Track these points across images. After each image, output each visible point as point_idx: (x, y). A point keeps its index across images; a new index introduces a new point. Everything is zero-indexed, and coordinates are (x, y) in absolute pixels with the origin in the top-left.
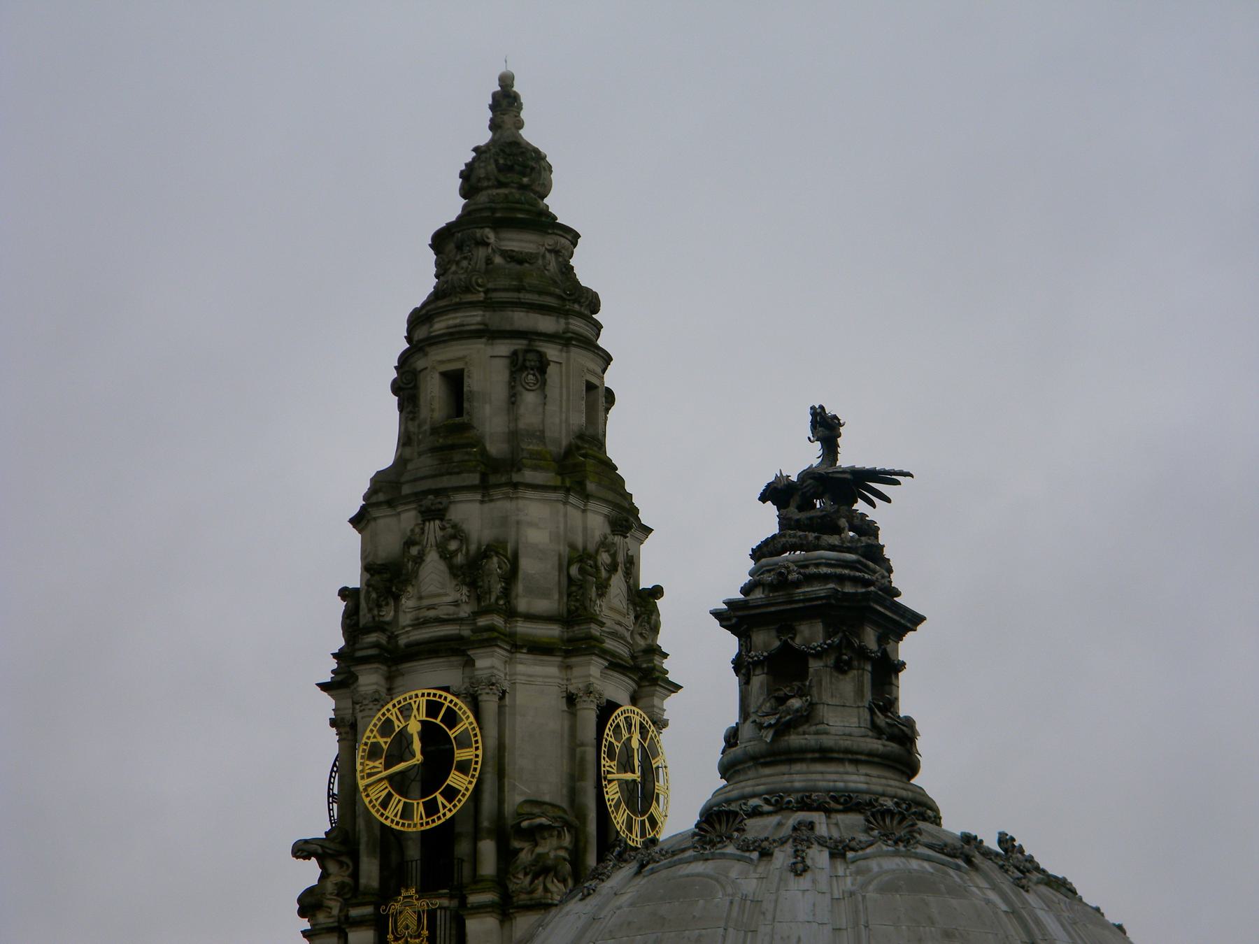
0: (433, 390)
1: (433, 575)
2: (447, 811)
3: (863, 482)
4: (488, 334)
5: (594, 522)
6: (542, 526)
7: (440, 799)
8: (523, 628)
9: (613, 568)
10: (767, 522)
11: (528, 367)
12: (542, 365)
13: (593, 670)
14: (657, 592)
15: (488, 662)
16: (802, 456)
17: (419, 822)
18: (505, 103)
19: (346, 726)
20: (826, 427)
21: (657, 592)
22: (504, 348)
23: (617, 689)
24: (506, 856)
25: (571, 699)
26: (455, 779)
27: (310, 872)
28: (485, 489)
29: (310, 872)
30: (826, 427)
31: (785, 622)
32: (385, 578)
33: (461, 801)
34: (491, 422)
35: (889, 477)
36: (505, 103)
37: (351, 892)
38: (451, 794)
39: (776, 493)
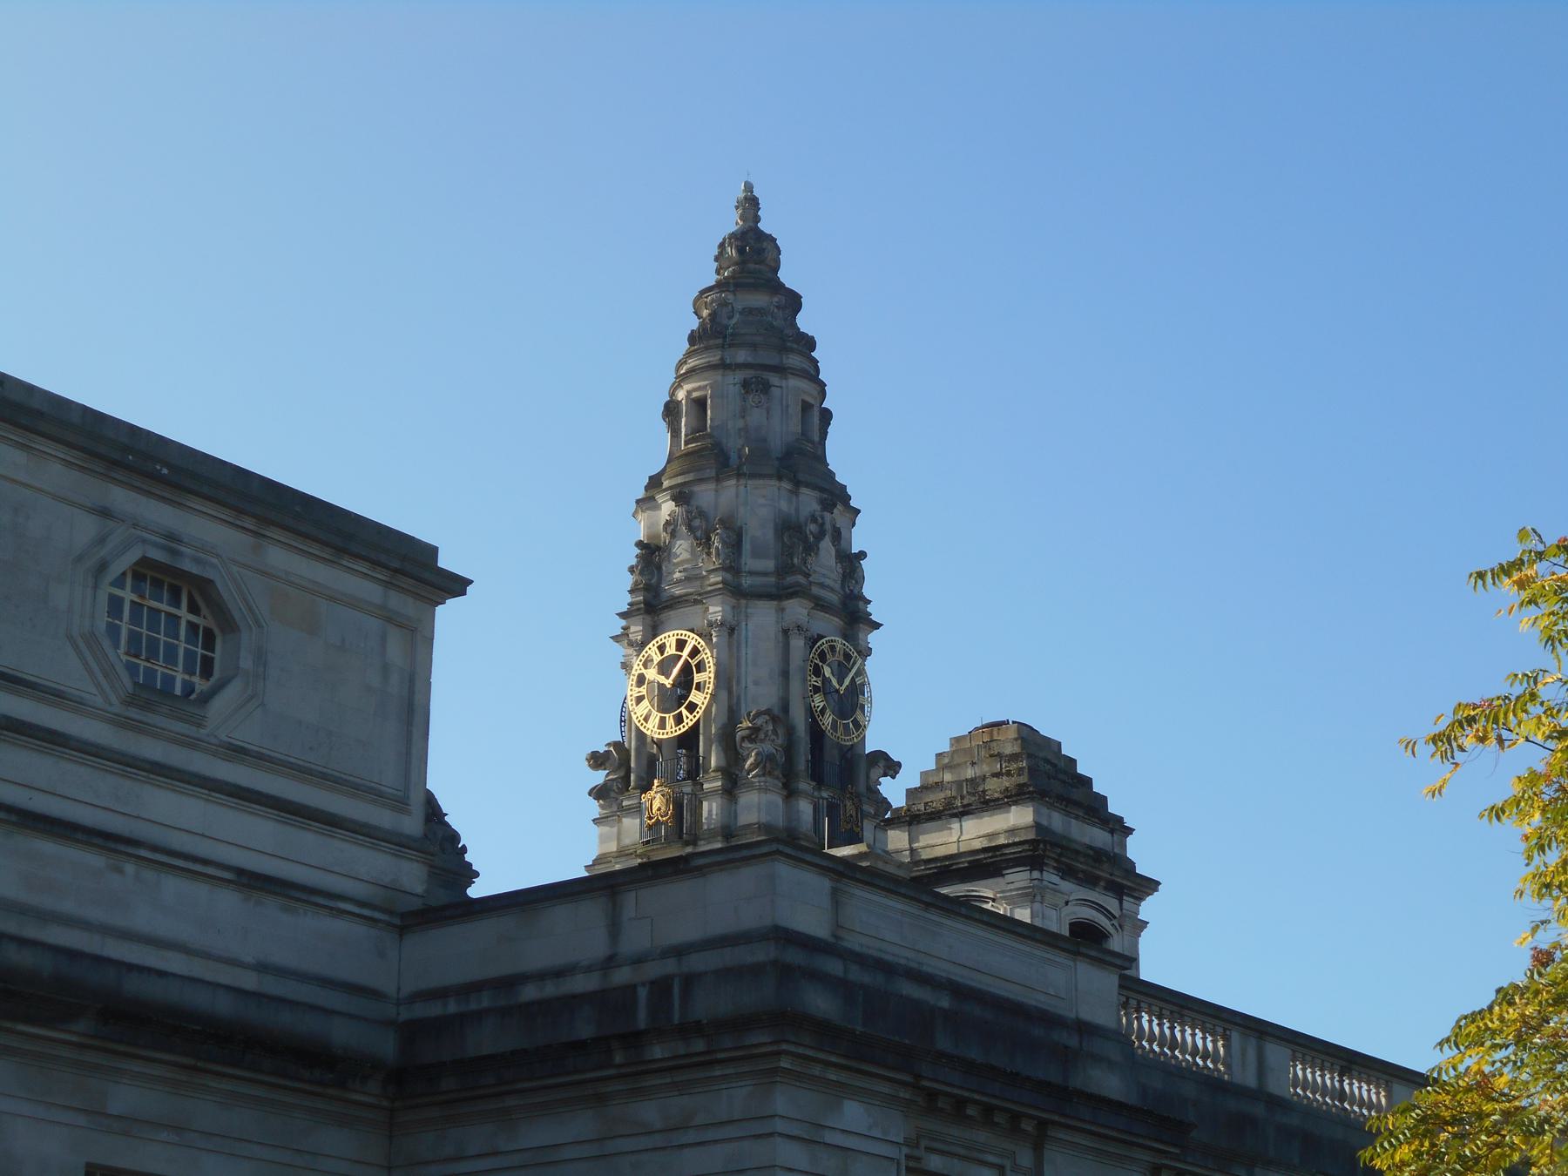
2: (689, 720)
5: (809, 501)
7: (685, 712)
8: (747, 582)
9: (820, 535)
11: (755, 387)
12: (766, 388)
13: (797, 610)
14: (862, 555)
17: (672, 731)
18: (750, 204)
21: (862, 555)
22: (739, 376)
23: (828, 626)
25: (786, 632)
26: (695, 697)
27: (600, 777)
29: (600, 777)
33: (699, 713)
36: (750, 204)
38: (692, 708)
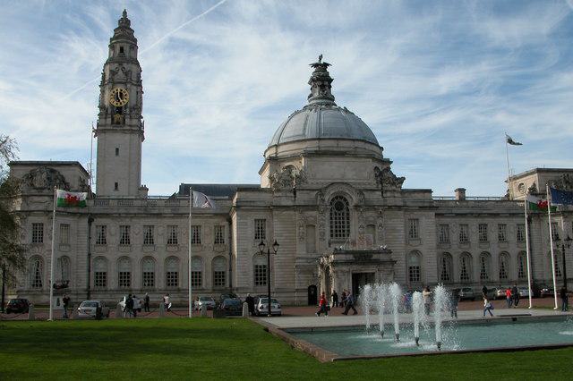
0: (118, 50)
1: (120, 72)
2: (123, 104)
3: (326, 65)
4: (127, 43)
6: (134, 68)
10: (314, 69)
15: (129, 85)
16: (317, 61)
18: (125, 13)
19: (103, 92)
20: (321, 58)
24: (131, 111)
28: (128, 63)
30: (321, 58)
31: (323, 81)
32: (113, 73)
34: (127, 54)
35: (328, 65)
36: (125, 13)
37: (107, 114)
39: (315, 65)
